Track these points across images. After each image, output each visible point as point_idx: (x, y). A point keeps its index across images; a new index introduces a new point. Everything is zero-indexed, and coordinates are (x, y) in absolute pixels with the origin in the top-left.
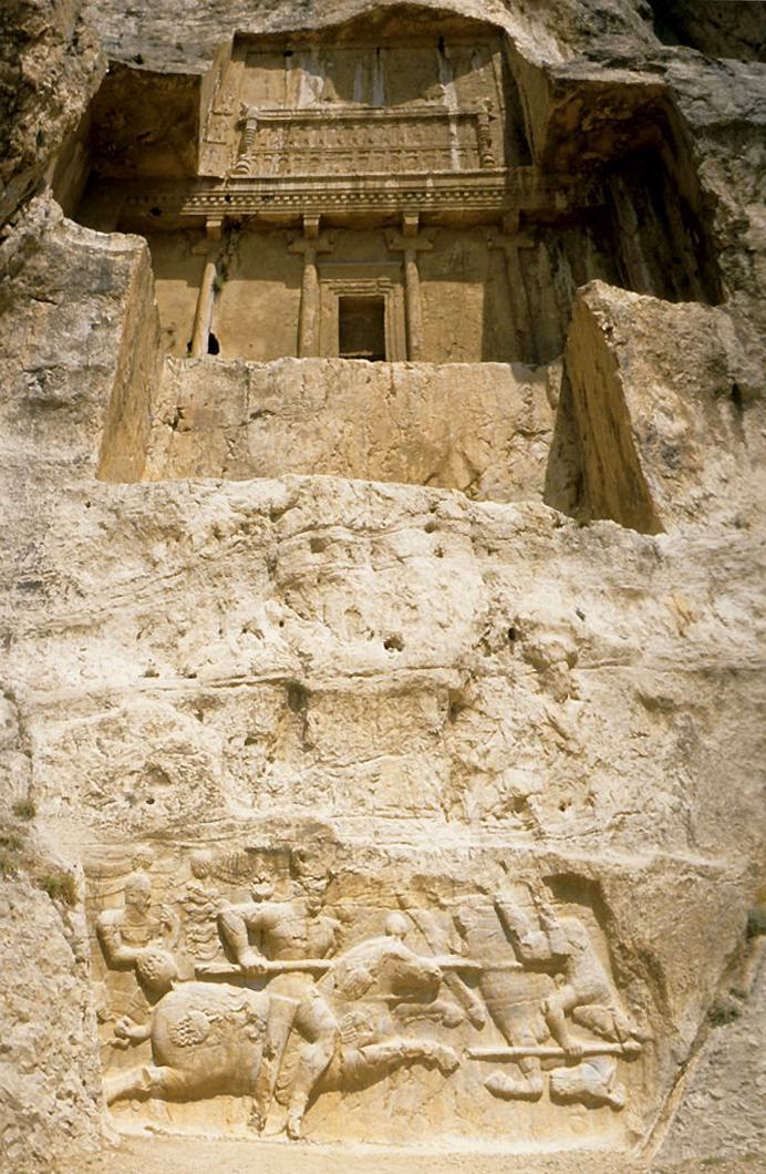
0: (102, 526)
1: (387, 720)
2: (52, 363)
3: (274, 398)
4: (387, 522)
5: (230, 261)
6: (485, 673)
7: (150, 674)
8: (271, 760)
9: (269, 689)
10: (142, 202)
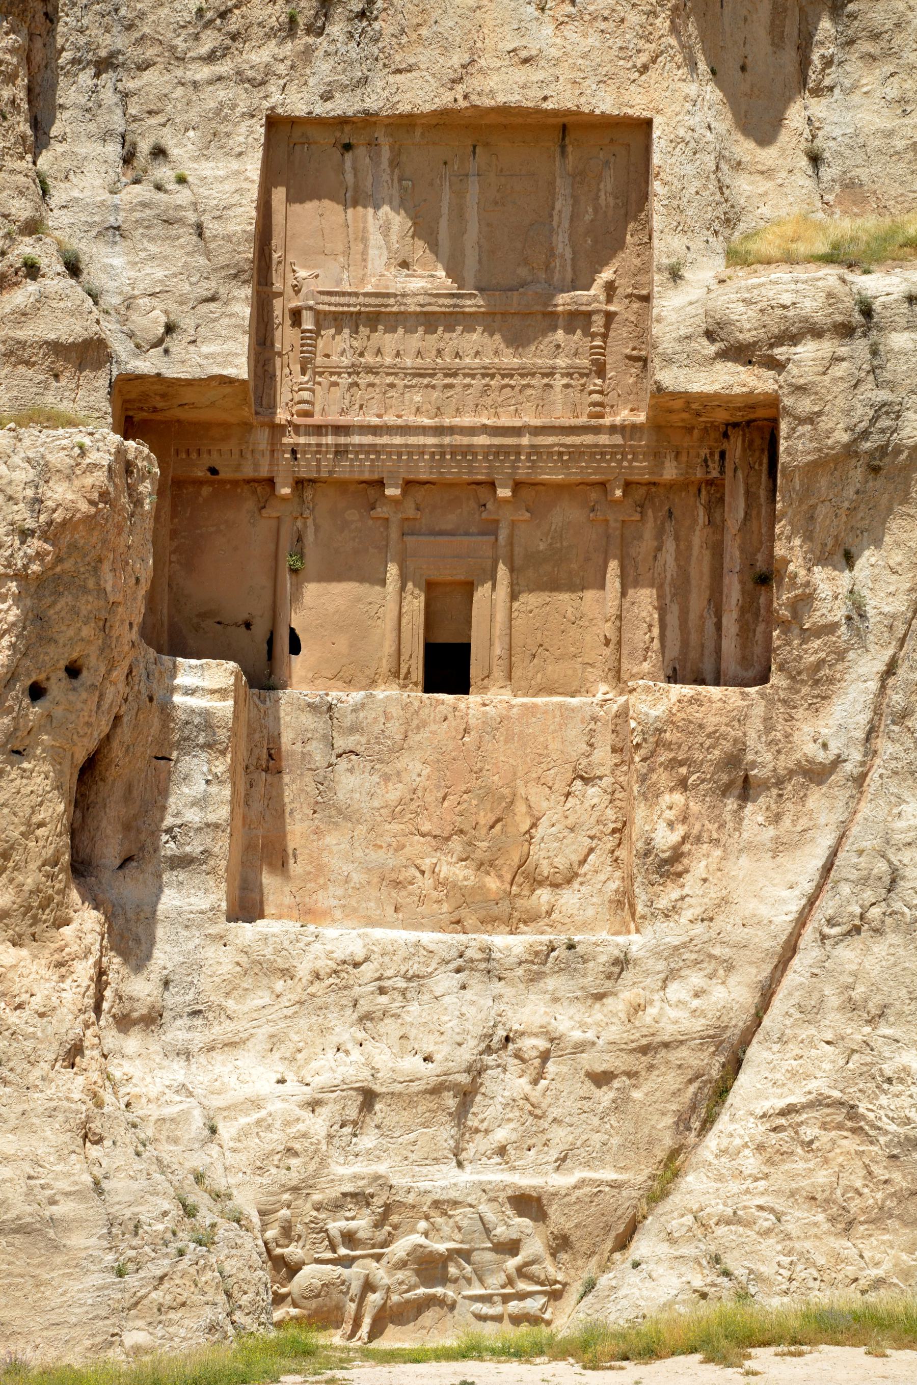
0: (238, 964)
1: (421, 1109)
2: (179, 822)
3: (357, 737)
4: (430, 970)
5: (305, 524)
6: (488, 1068)
7: (281, 1081)
8: (355, 1135)
9: (353, 1093)
10: (194, 456)
